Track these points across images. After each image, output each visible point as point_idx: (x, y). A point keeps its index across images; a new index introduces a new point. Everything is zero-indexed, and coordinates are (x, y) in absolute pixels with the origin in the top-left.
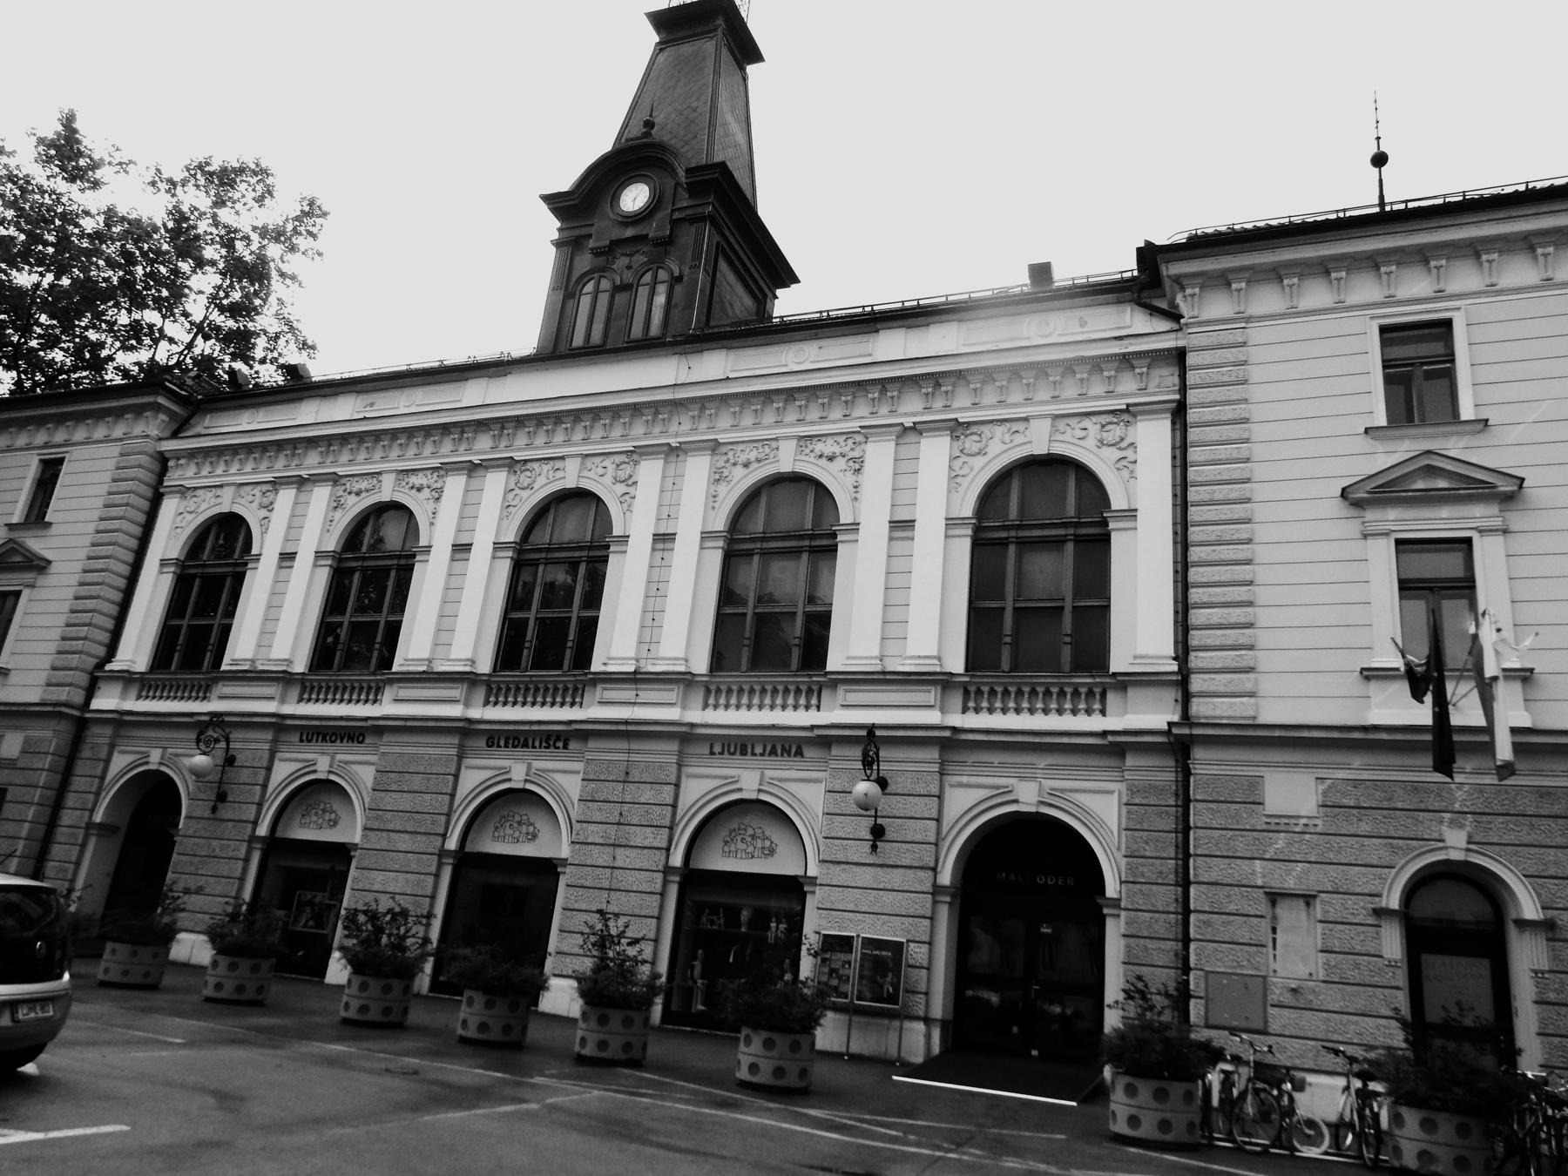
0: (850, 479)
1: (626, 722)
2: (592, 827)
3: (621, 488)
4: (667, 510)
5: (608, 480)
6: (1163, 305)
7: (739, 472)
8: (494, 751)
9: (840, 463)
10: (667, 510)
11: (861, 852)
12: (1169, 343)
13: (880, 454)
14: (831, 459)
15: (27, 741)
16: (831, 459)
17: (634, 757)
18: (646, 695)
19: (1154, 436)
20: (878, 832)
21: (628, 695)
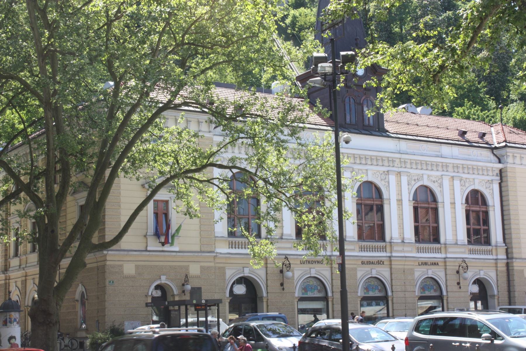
0: (439, 189)
1: (406, 257)
2: (398, 287)
3: (383, 183)
4: (400, 193)
5: (379, 179)
6: (495, 152)
7: (413, 182)
8: (364, 265)
9: (436, 184)
10: (400, 193)
11: (456, 288)
12: (500, 166)
13: (446, 182)
14: (434, 182)
15: (202, 268)
16: (434, 182)
17: (406, 267)
18: (406, 249)
19: (496, 187)
20: (458, 284)
21: (400, 248)
